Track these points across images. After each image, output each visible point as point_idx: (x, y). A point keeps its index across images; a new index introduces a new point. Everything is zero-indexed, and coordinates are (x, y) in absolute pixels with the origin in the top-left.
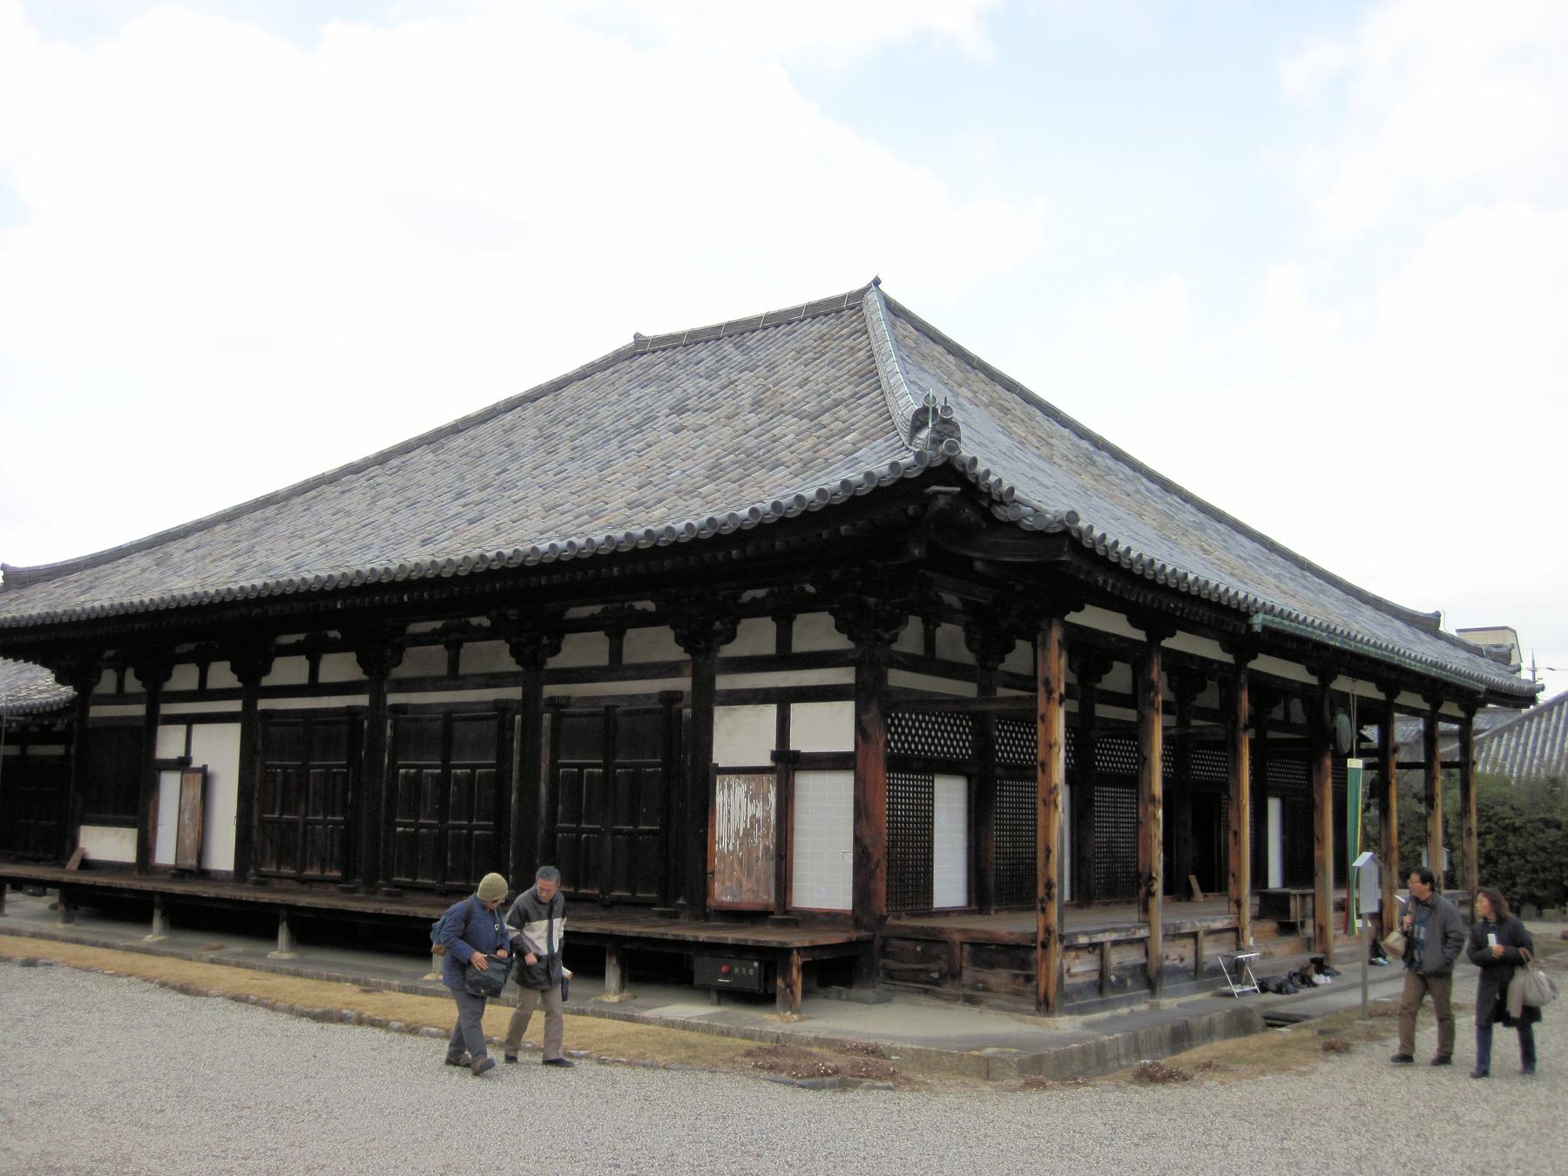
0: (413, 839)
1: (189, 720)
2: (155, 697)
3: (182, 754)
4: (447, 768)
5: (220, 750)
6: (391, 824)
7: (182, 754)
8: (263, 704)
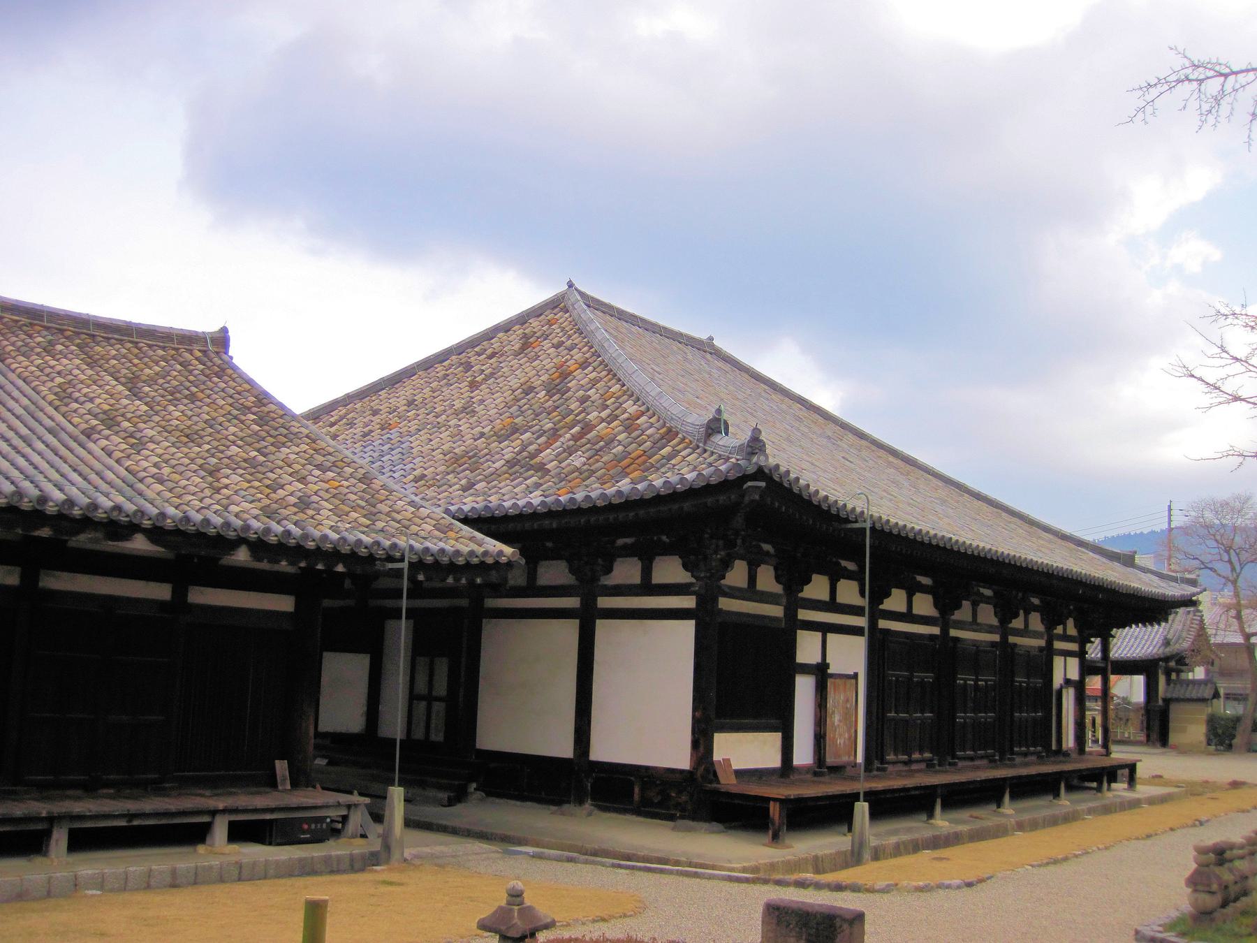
0: (964, 725)
1: (825, 629)
2: (793, 603)
3: (819, 660)
4: (977, 680)
5: (849, 656)
6: (954, 718)
7: (819, 660)
8: (883, 624)
